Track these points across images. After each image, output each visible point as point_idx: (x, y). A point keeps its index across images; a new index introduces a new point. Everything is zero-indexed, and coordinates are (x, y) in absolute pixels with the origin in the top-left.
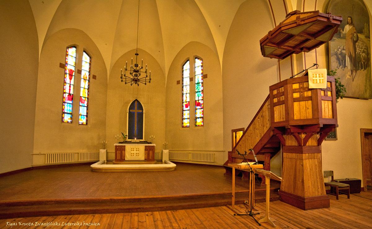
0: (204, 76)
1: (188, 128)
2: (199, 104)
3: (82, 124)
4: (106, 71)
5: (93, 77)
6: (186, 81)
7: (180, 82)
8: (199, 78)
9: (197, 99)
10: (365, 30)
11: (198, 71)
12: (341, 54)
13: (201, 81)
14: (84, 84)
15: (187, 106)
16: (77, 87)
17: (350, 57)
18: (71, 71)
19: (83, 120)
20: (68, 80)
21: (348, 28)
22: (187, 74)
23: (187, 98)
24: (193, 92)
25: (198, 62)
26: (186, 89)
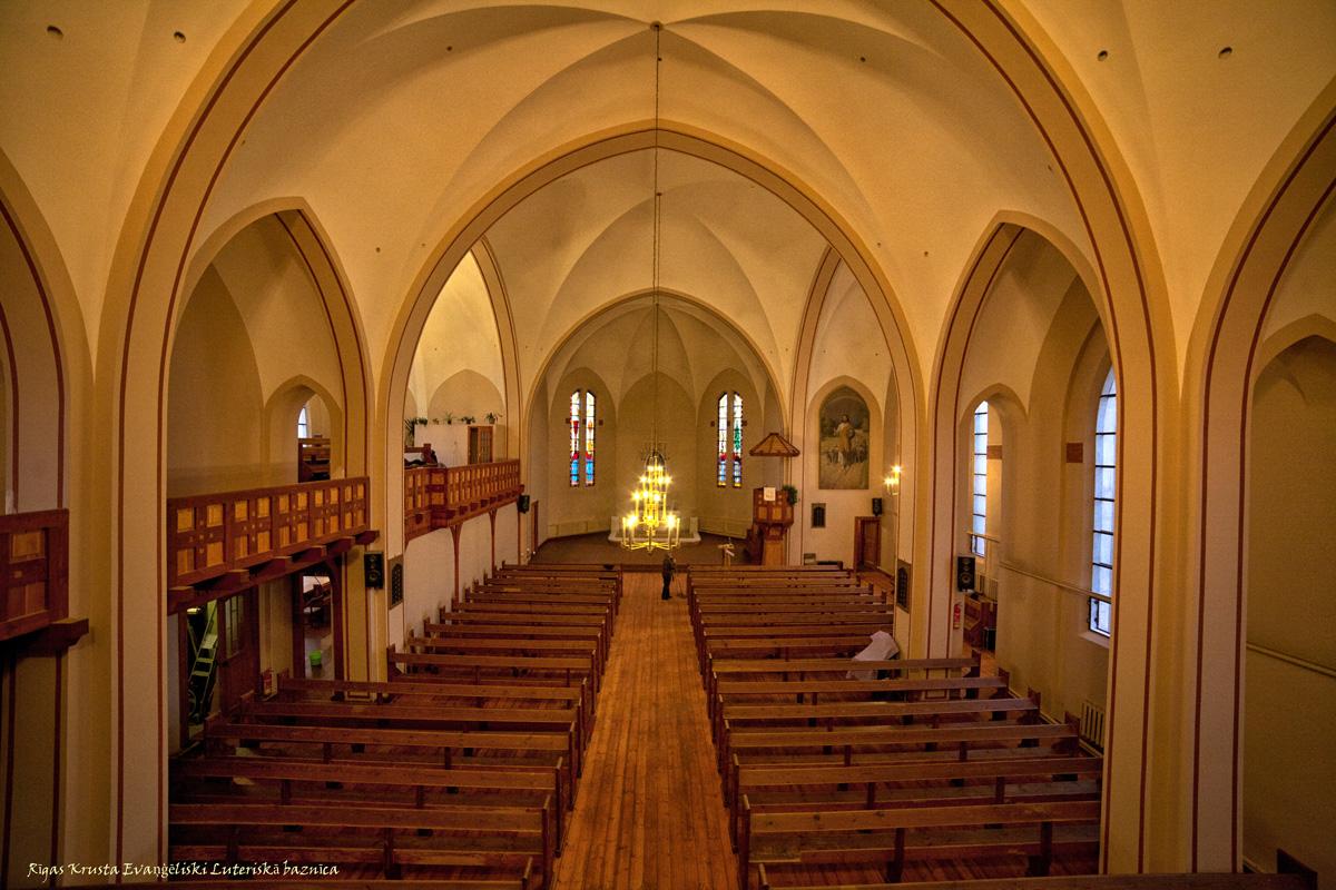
0: (744, 423)
1: (723, 490)
2: (737, 459)
3: (590, 485)
4: (614, 408)
5: (599, 422)
6: (723, 424)
7: (715, 424)
8: (738, 423)
9: (735, 451)
10: (864, 425)
11: (738, 412)
12: (833, 451)
13: (740, 427)
14: (590, 435)
15: (723, 460)
16: (582, 441)
17: (844, 453)
18: (576, 423)
19: (590, 481)
20: (573, 437)
21: (842, 426)
22: (723, 413)
23: (723, 448)
24: (730, 442)
25: (738, 401)
26: (723, 435)
